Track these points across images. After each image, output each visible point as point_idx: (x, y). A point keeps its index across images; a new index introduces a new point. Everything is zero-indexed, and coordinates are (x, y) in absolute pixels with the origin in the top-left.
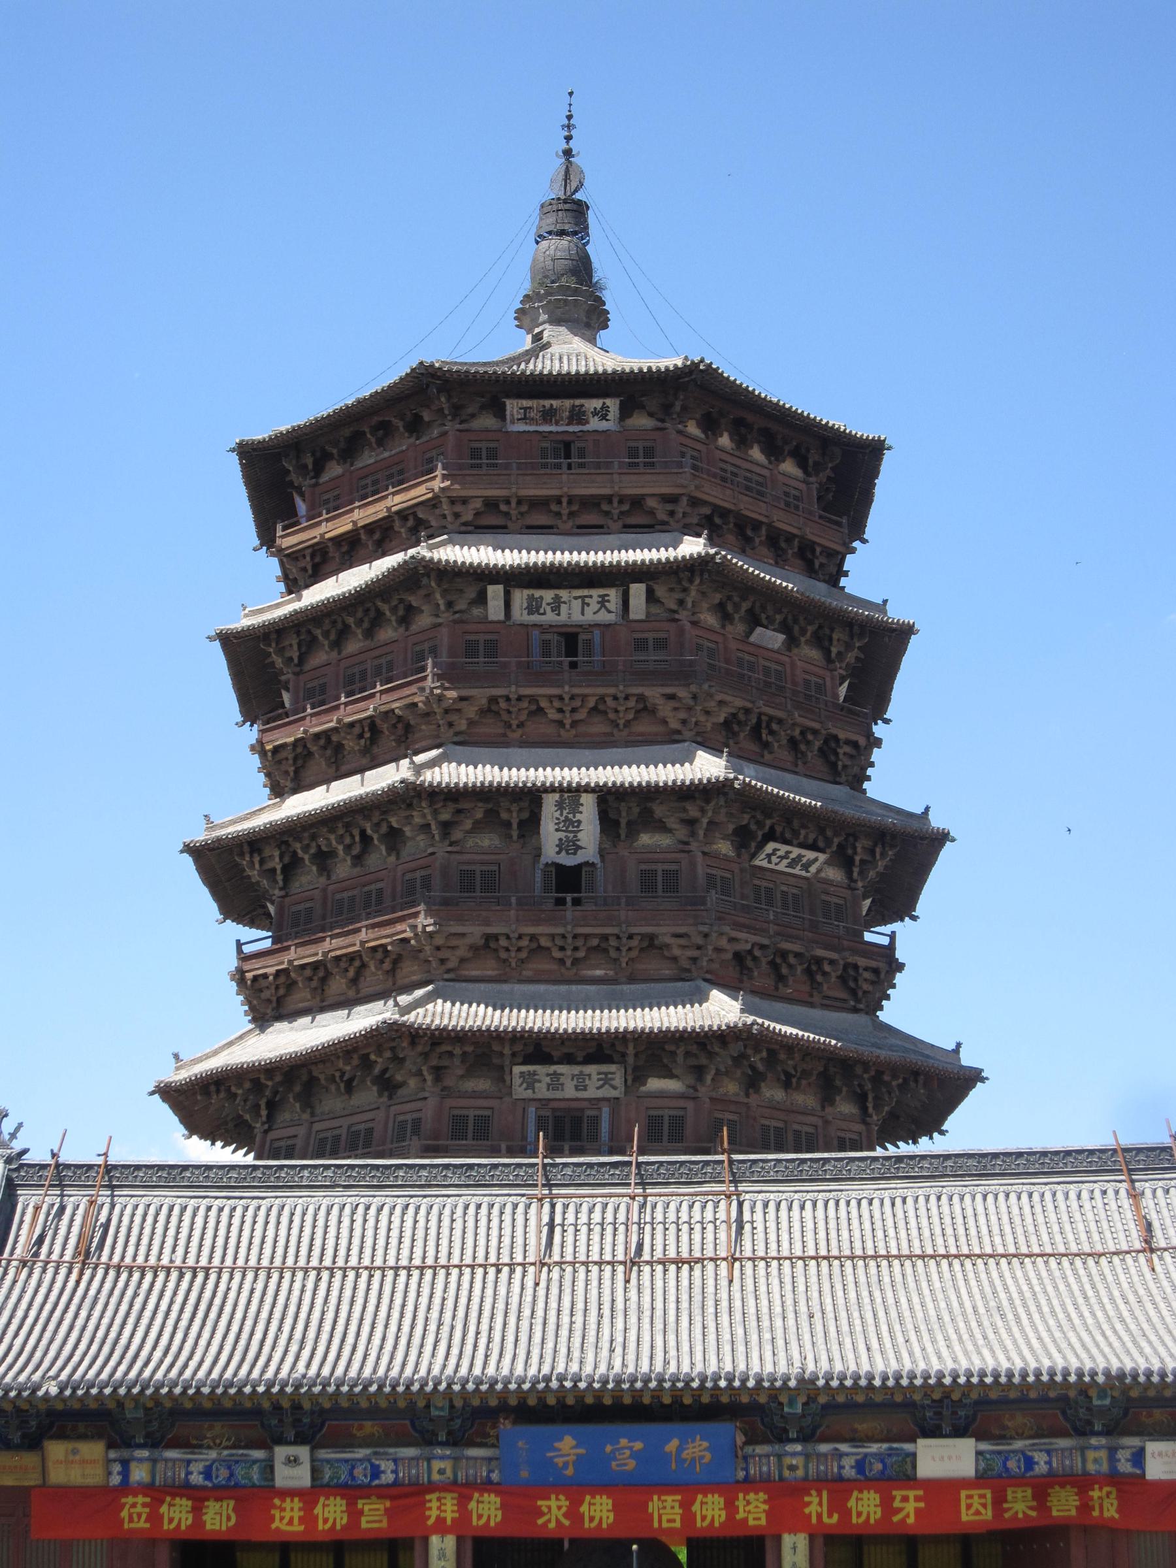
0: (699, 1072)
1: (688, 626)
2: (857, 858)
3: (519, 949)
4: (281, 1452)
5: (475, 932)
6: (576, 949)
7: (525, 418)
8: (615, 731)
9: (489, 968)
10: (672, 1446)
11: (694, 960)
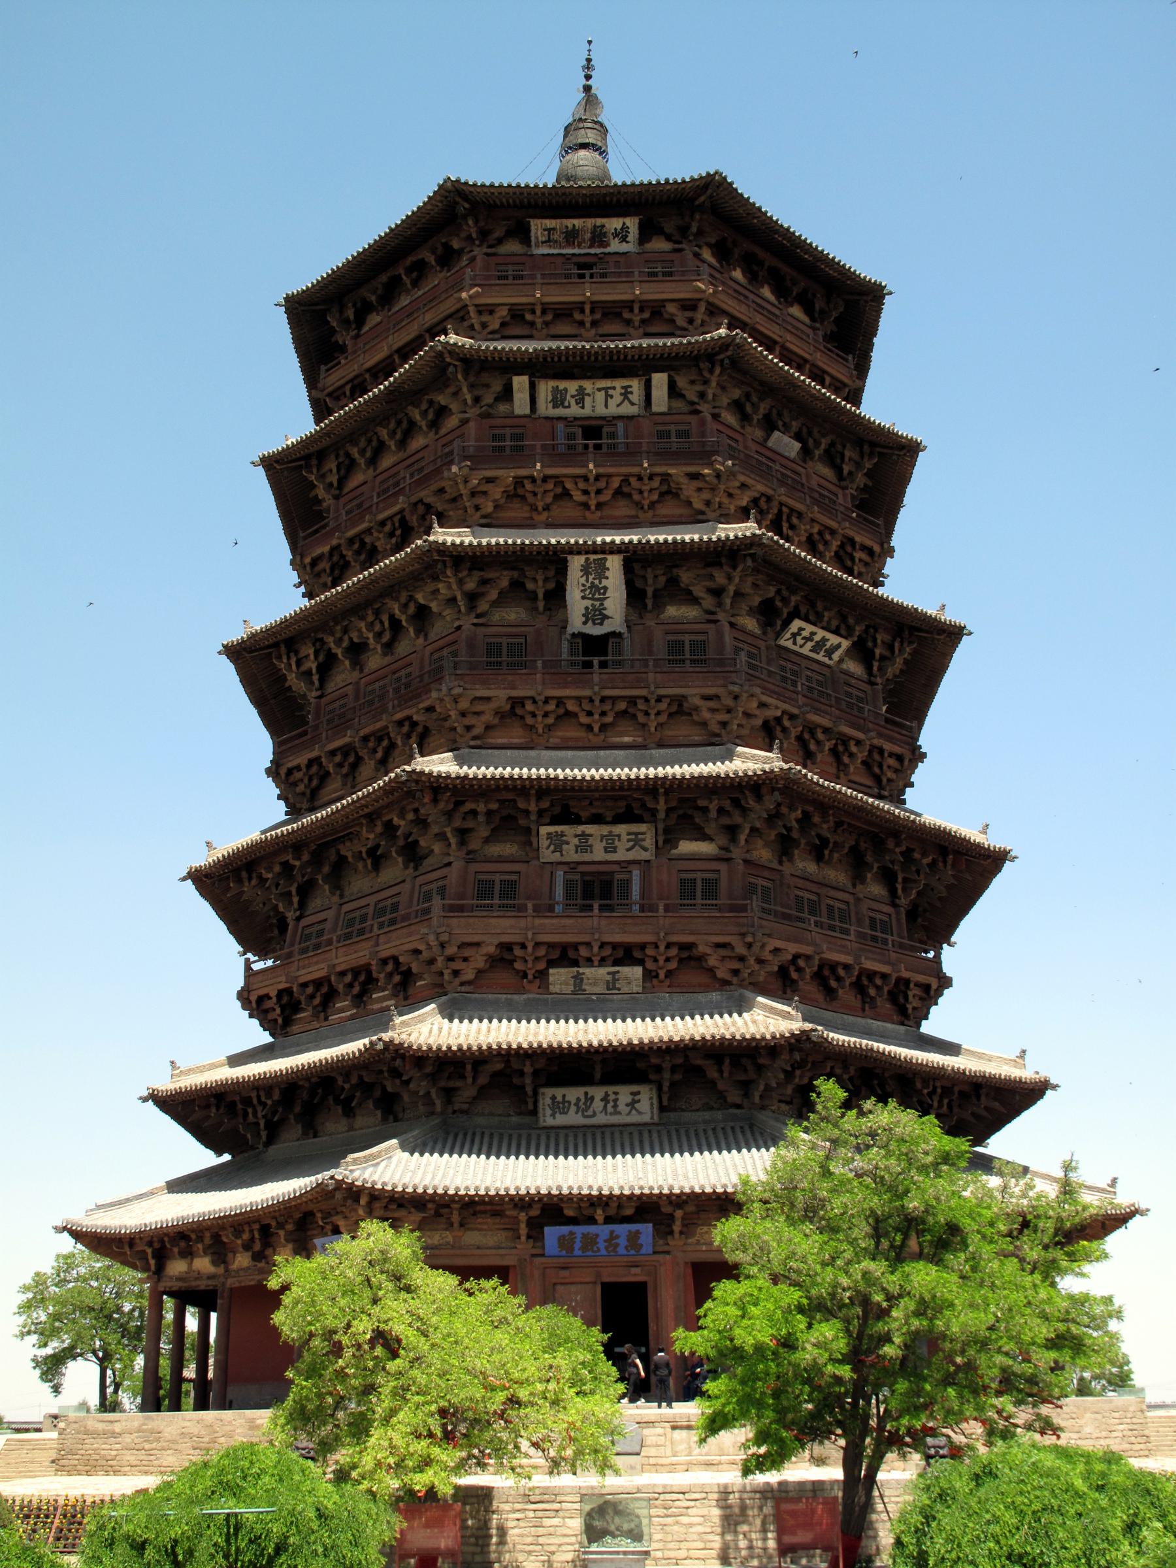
0: (732, 831)
1: (709, 418)
2: (877, 652)
3: (546, 715)
5: (500, 695)
6: (603, 714)
7: (549, 241)
8: (641, 514)
9: (516, 734)
11: (724, 724)
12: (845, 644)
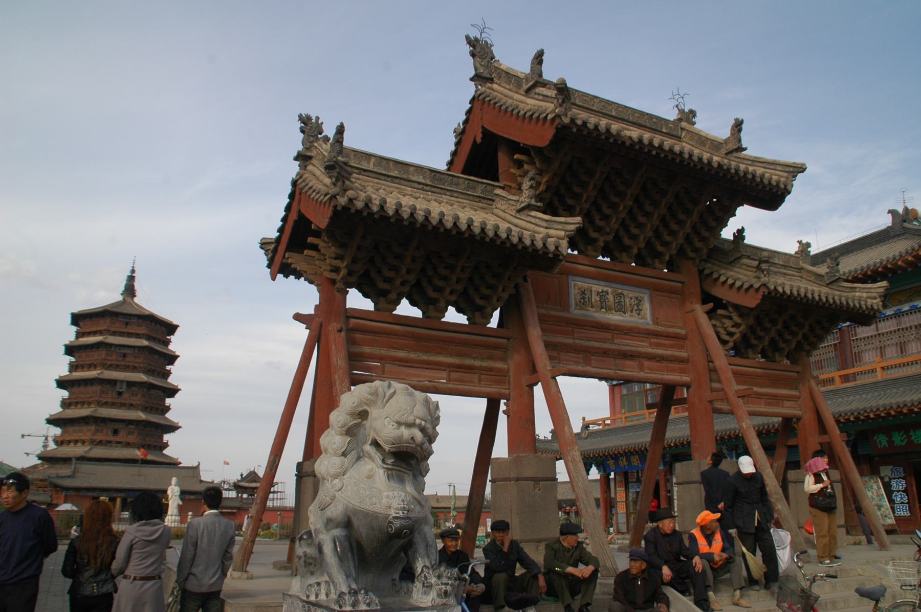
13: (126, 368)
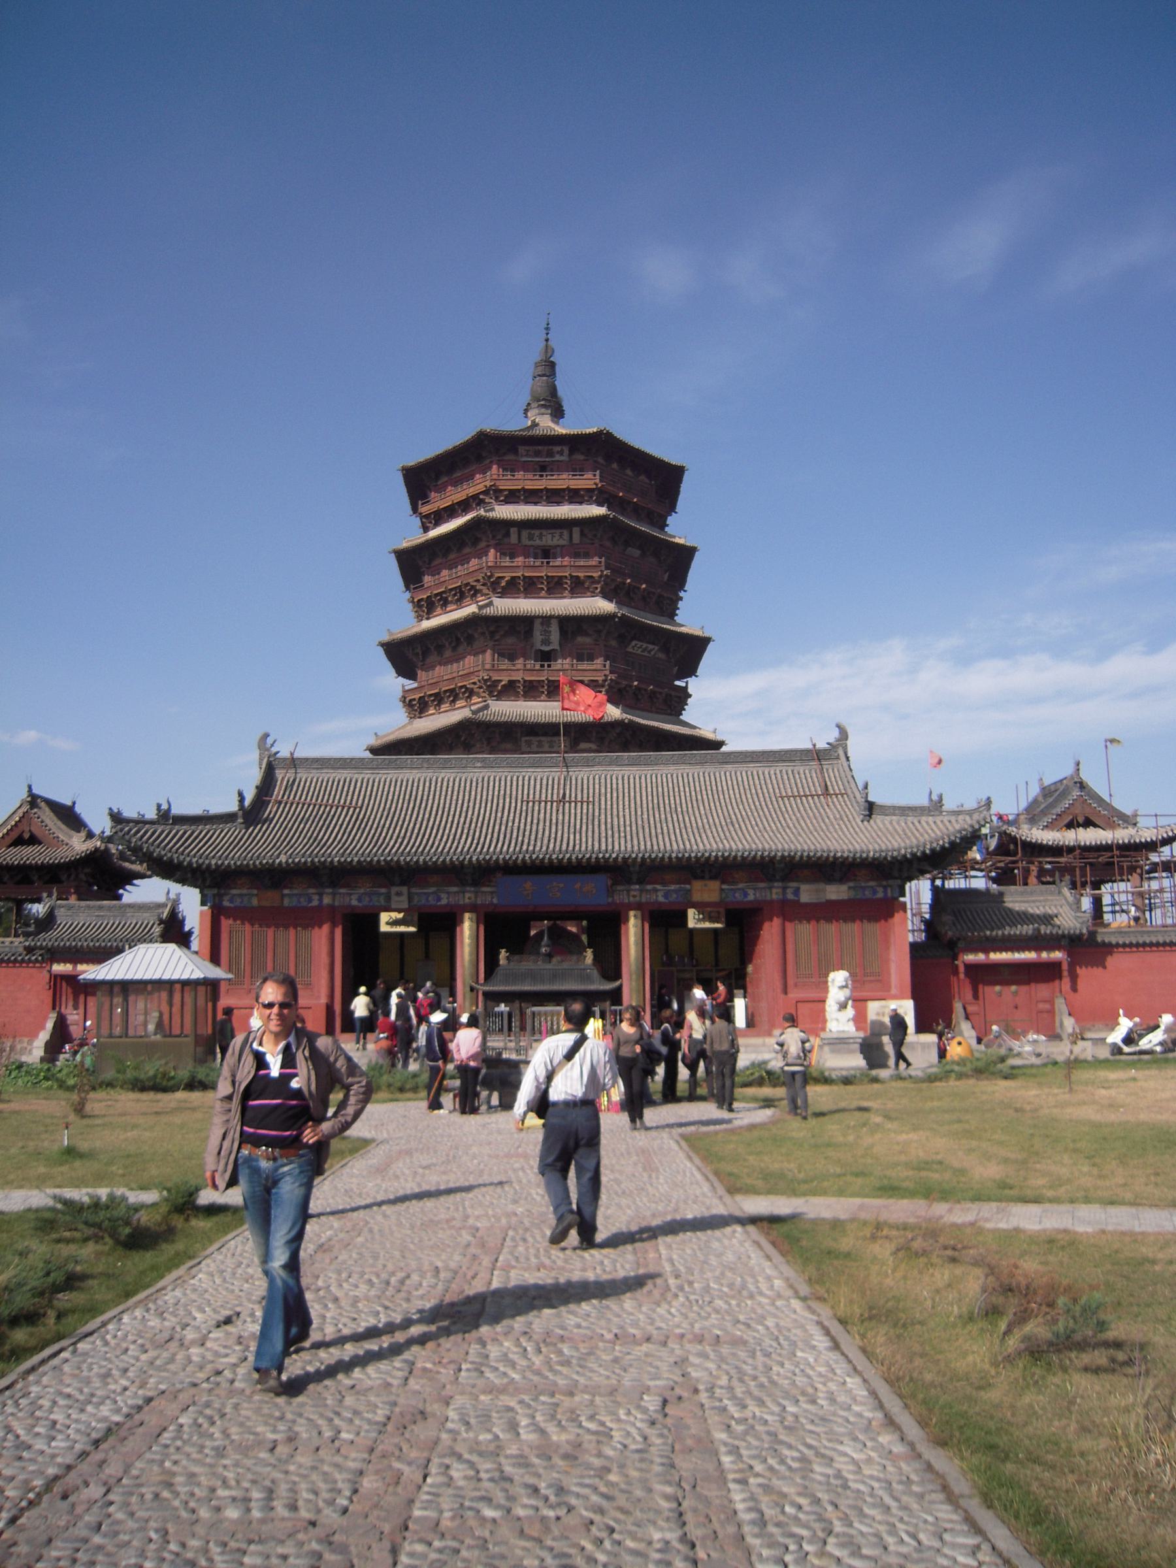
4: (394, 889)
10: (578, 886)
12: (657, 648)
13: (555, 587)
